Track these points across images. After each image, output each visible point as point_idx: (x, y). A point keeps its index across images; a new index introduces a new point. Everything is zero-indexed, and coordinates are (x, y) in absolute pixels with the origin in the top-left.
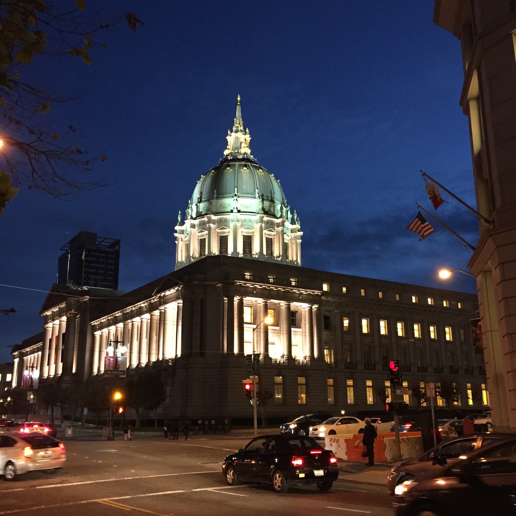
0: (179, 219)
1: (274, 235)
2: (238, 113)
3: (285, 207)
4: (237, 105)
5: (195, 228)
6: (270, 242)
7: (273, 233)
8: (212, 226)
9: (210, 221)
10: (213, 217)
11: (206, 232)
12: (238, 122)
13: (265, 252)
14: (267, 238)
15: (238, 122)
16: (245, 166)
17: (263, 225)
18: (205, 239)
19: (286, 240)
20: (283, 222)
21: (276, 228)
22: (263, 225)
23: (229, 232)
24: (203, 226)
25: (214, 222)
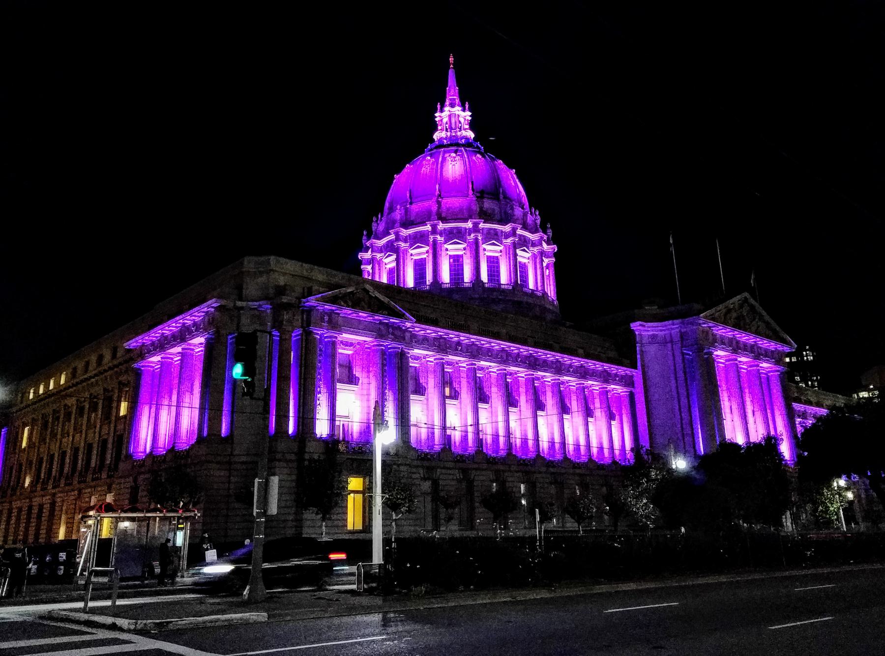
1: (501, 251)
4: (449, 68)
5: (381, 252)
6: (493, 264)
7: (498, 248)
8: (403, 245)
10: (405, 232)
11: (394, 257)
13: (484, 277)
14: (489, 258)
16: (456, 152)
17: (480, 238)
20: (514, 230)
21: (504, 241)
23: (427, 252)
24: (390, 248)
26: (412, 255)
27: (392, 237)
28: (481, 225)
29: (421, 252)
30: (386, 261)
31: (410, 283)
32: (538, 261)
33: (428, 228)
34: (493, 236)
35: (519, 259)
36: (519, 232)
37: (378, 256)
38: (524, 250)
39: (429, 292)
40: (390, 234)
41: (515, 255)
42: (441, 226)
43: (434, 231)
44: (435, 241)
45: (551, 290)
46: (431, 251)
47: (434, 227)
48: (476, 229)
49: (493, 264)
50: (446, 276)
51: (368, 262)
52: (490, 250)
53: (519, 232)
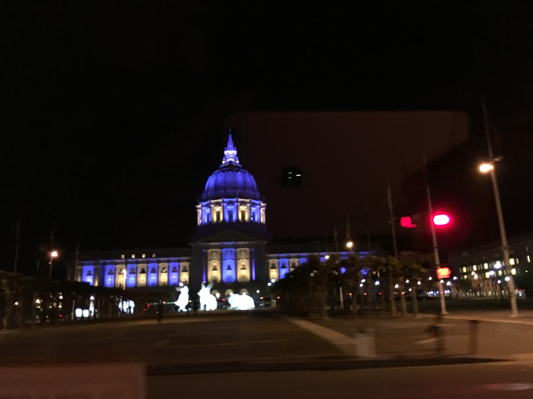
0: (198, 200)
2: (230, 139)
3: (254, 191)
6: (243, 213)
8: (212, 206)
9: (211, 203)
10: (213, 201)
12: (230, 144)
15: (230, 144)
22: (239, 204)
24: (208, 206)
25: (213, 204)
29: (219, 209)
31: (215, 219)
34: (243, 203)
35: (253, 211)
36: (253, 201)
37: (204, 208)
39: (220, 223)
41: (251, 209)
45: (263, 220)
49: (243, 213)
50: (227, 217)
51: (200, 209)
52: (243, 208)
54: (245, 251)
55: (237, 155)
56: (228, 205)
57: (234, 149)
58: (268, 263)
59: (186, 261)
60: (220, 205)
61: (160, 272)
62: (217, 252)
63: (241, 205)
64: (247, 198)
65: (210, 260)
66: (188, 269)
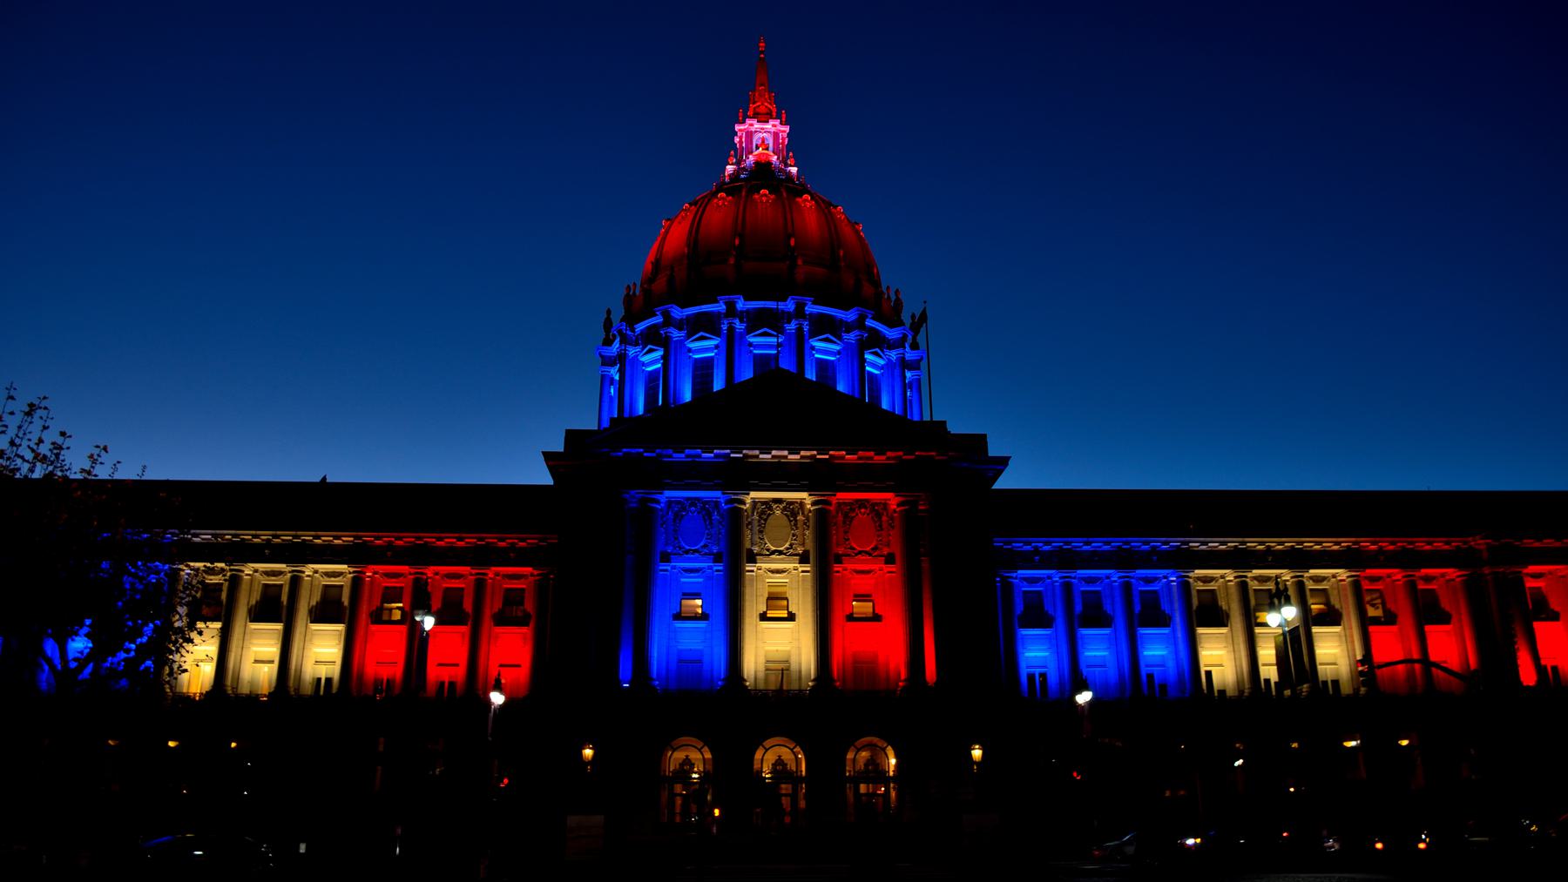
1: (839, 352)
8: (676, 334)
10: (678, 313)
11: (659, 353)
18: (657, 370)
19: (873, 365)
21: (846, 337)
23: (717, 347)
26: (690, 350)
27: (658, 319)
28: (811, 309)
29: (704, 347)
30: (646, 359)
32: (897, 372)
33: (720, 307)
36: (870, 323)
37: (632, 351)
38: (876, 354)
40: (654, 315)
42: (741, 305)
43: (731, 311)
44: (731, 328)
46: (723, 348)
47: (731, 306)
48: (799, 312)
53: (870, 323)
54: (877, 510)
55: (789, 148)
56: (749, 330)
57: (778, 117)
58: (1008, 587)
59: (521, 558)
60: (716, 332)
61: (363, 617)
62: (707, 508)
63: (814, 333)
64: (845, 307)
65: (666, 558)
66: (529, 606)
